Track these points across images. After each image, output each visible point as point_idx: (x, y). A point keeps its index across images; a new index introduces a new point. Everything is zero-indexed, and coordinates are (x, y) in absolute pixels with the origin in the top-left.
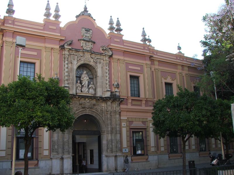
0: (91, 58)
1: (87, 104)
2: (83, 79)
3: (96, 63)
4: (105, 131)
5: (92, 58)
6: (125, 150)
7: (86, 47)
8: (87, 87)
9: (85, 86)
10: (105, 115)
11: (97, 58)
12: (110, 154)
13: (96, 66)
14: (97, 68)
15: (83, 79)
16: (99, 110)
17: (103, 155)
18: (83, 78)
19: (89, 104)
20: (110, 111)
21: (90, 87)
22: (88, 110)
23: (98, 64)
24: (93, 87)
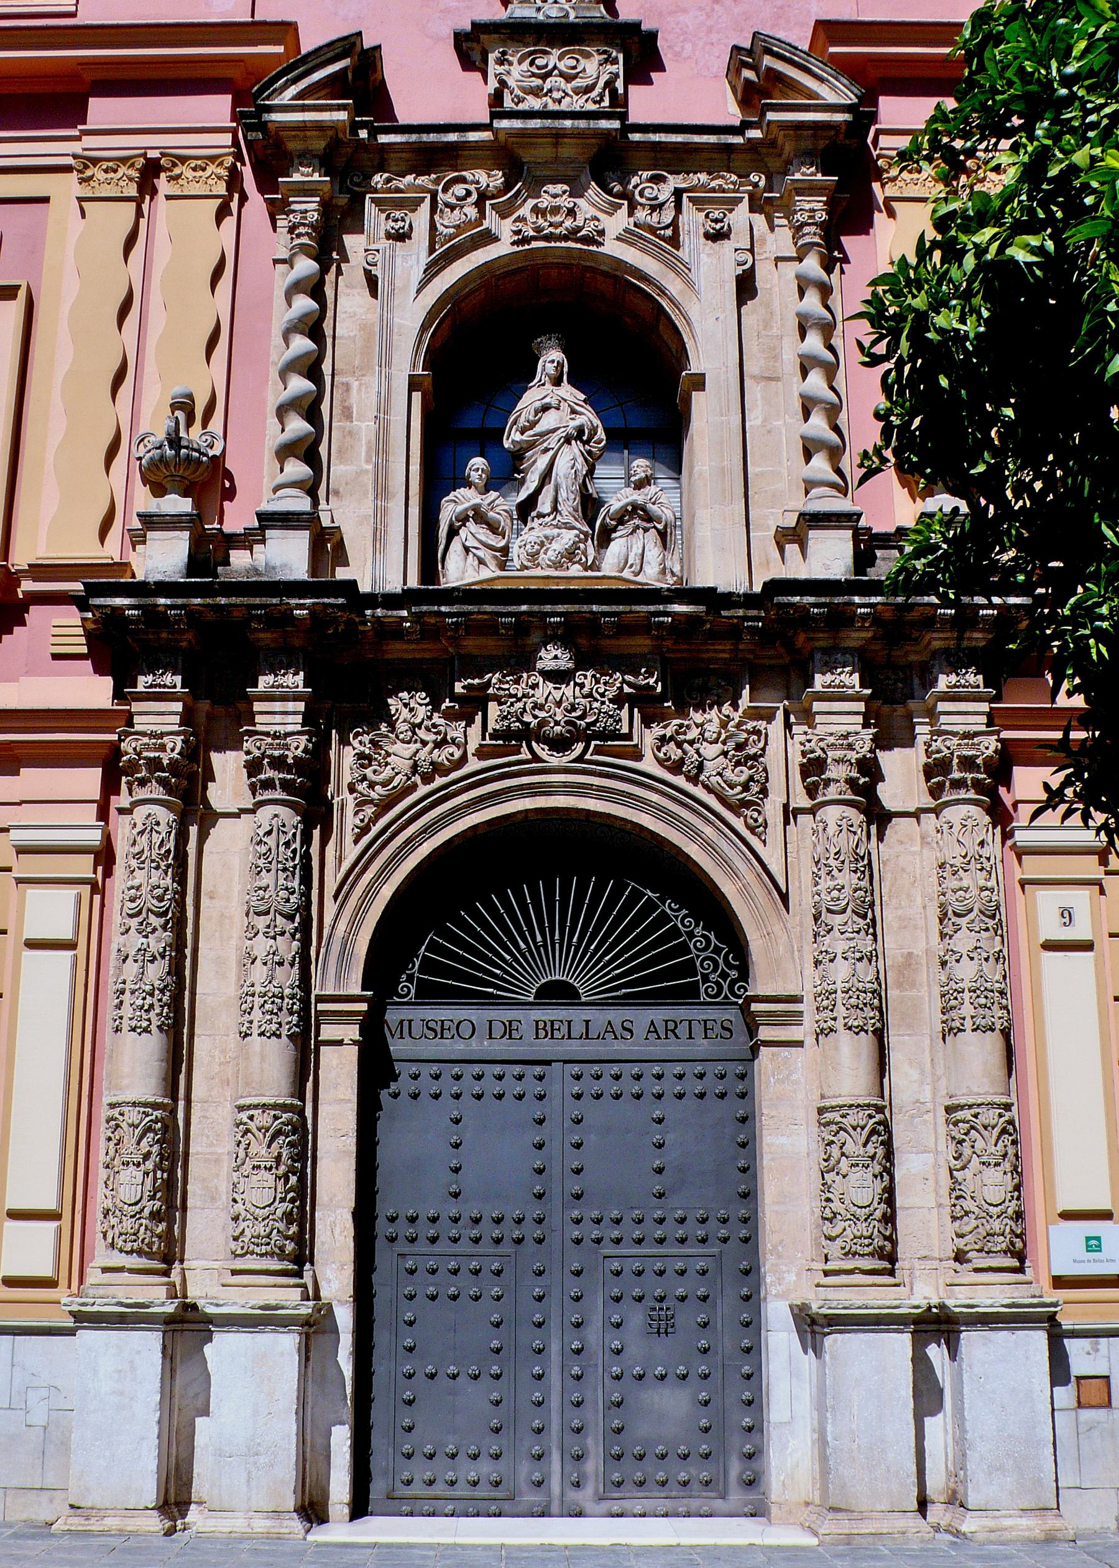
1: (546, 689)
4: (796, 999)
7: (536, 92)
9: (544, 504)
10: (789, 814)
11: (678, 193)
13: (681, 269)
14: (689, 284)
16: (710, 751)
21: (622, 518)
22: (555, 760)
23: (693, 244)
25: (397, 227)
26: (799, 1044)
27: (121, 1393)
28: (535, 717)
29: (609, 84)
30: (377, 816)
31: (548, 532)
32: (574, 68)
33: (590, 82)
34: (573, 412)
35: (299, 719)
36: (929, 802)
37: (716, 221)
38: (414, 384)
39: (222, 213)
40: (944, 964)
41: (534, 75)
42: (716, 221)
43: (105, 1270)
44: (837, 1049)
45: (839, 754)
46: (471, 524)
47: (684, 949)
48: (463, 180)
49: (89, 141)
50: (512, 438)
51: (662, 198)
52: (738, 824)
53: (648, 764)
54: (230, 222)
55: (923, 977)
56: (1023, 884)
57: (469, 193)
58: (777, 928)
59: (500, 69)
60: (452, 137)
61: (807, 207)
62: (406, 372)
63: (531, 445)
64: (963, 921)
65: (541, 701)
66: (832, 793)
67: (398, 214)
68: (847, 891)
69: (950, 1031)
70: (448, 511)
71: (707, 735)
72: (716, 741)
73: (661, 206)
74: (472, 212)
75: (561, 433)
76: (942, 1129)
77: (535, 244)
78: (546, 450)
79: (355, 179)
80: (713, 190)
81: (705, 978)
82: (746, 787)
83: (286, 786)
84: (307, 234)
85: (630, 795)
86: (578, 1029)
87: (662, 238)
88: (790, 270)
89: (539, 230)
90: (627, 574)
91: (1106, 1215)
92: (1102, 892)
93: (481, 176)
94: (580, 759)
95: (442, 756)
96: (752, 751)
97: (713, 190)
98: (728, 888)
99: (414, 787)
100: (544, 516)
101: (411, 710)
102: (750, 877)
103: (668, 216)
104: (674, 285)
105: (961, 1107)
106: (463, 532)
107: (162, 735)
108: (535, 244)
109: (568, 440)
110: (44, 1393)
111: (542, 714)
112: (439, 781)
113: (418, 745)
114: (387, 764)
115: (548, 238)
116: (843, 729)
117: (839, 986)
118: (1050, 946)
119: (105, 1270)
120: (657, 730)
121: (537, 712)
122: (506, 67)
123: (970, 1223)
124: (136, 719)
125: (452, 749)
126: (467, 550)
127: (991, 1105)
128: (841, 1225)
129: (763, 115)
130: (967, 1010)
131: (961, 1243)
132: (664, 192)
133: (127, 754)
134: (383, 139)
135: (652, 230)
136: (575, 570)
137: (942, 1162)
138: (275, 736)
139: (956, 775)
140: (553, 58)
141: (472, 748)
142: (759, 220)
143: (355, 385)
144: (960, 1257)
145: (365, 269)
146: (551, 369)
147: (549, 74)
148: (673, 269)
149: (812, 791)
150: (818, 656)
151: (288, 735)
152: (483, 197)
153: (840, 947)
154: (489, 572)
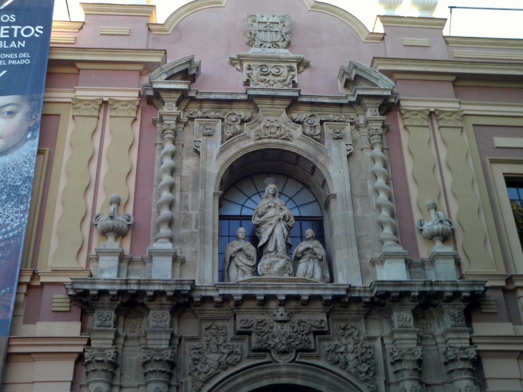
0: (294, 121)
2: (262, 219)
3: (319, 139)
5: (299, 122)
9: (271, 247)
11: (322, 122)
14: (328, 158)
15: (262, 219)
18: (260, 216)
19: (287, 328)
20: (413, 354)
21: (303, 254)
22: (283, 360)
24: (317, 250)
25: (208, 132)
28: (273, 341)
31: (273, 259)
32: (278, 72)
33: (285, 78)
34: (281, 209)
37: (338, 133)
38: (215, 194)
41: (262, 75)
42: (338, 133)
51: (315, 124)
57: (237, 120)
59: (248, 72)
61: (375, 128)
63: (264, 222)
65: (276, 334)
66: (406, 375)
71: (349, 349)
72: (352, 352)
73: (315, 127)
74: (238, 127)
75: (277, 218)
78: (271, 224)
79: (191, 113)
80: (335, 121)
84: (171, 133)
87: (316, 139)
90: (307, 277)
96: (369, 357)
97: (335, 121)
100: (271, 252)
101: (217, 338)
103: (318, 132)
104: (321, 159)
106: (236, 260)
107: (104, 349)
111: (277, 340)
113: (220, 355)
114: (206, 363)
116: (409, 346)
121: (273, 339)
122: (251, 71)
124: (93, 342)
126: (237, 266)
129: (355, 92)
132: (317, 123)
133: (87, 358)
135: (312, 136)
136: (286, 276)
141: (246, 355)
143: (190, 196)
145: (194, 149)
146: (271, 191)
147: (268, 74)
151: (162, 350)
152: (243, 122)
154: (249, 277)
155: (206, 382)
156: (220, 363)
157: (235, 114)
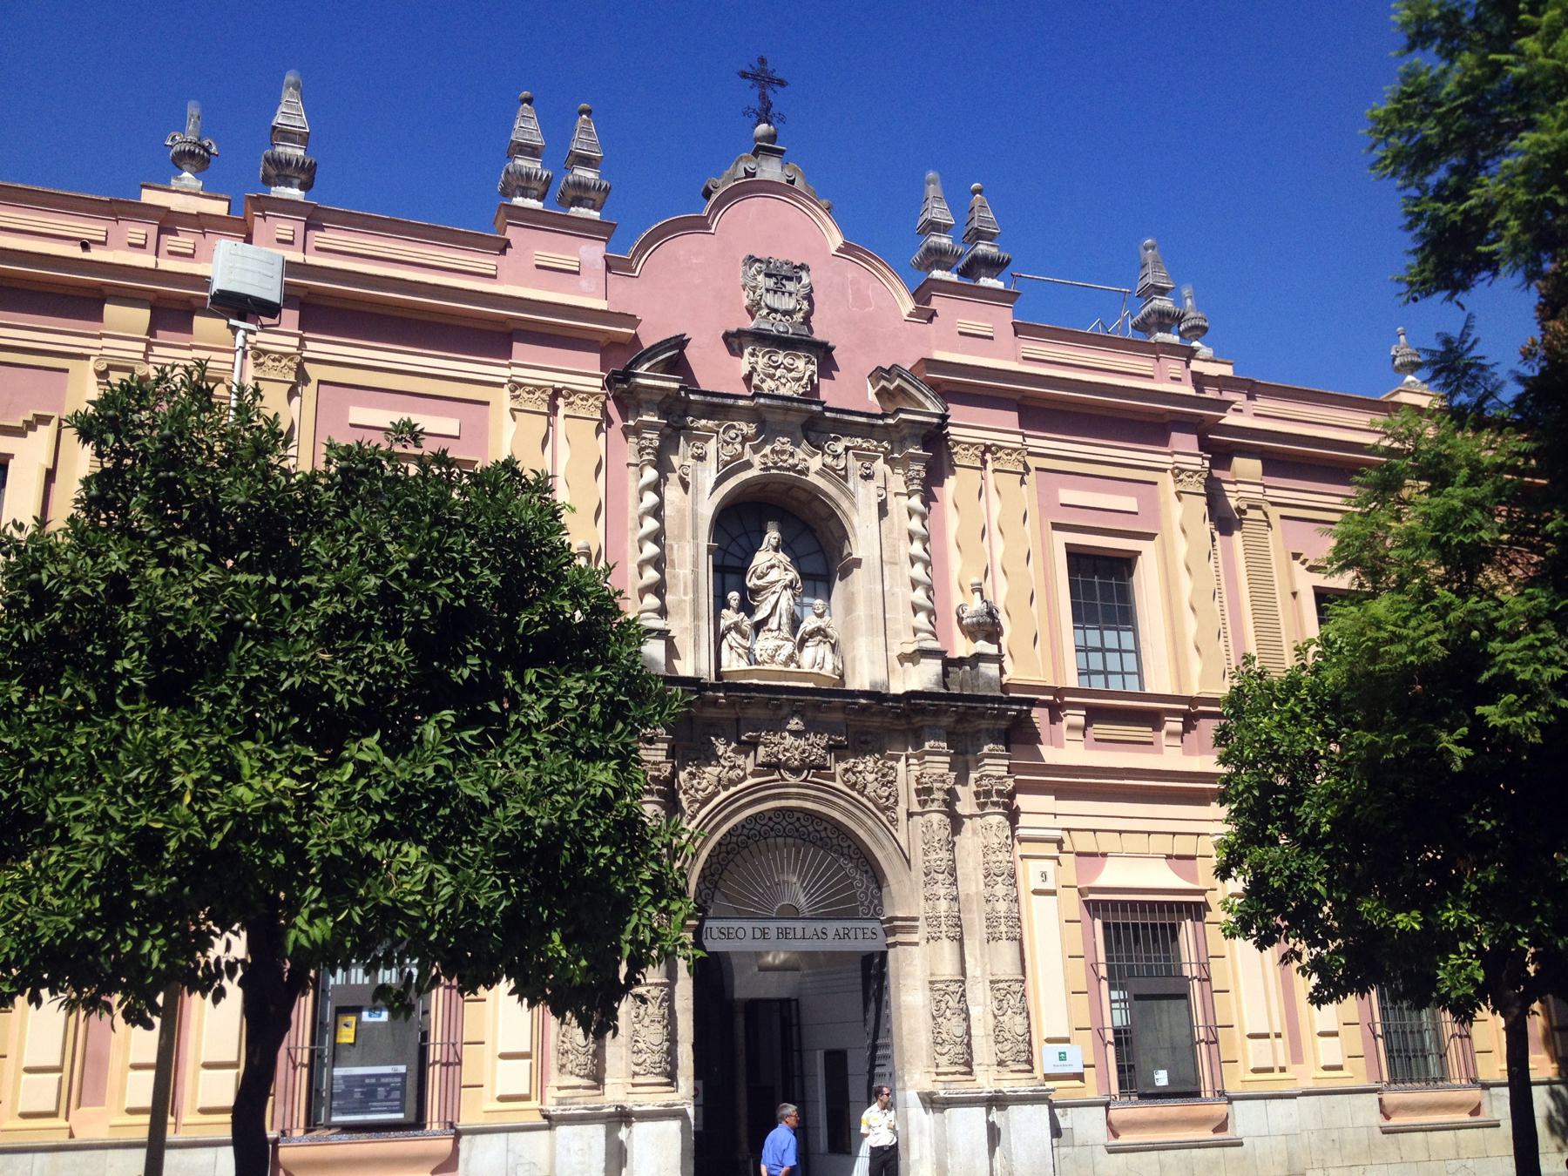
4: (915, 919)
6: (1062, 1056)
7: (772, 377)
8: (785, 628)
9: (773, 623)
10: (910, 815)
11: (847, 449)
12: (953, 1085)
13: (850, 495)
14: (854, 504)
17: (903, 1089)
18: (759, 578)
21: (812, 634)
22: (792, 780)
23: (854, 483)
26: (916, 944)
27: (583, 1163)
29: (811, 377)
30: (700, 809)
34: (786, 569)
35: (664, 753)
36: (977, 811)
39: (598, 430)
40: (988, 901)
43: (559, 1088)
44: (942, 948)
45: (939, 785)
46: (733, 633)
47: (851, 886)
48: (734, 427)
49: (515, 371)
50: (752, 582)
52: (884, 818)
53: (839, 784)
54: (602, 435)
55: (975, 907)
56: (1022, 857)
58: (905, 878)
59: (753, 360)
60: (730, 401)
62: (706, 543)
64: (1000, 879)
66: (935, 806)
67: (698, 444)
68: (945, 861)
69: (992, 938)
70: (724, 624)
74: (739, 447)
75: (782, 583)
76: (989, 993)
77: (773, 471)
80: (864, 449)
81: (862, 904)
82: (888, 799)
83: (659, 792)
85: (830, 801)
86: (799, 934)
88: (904, 500)
89: (775, 463)
91: (1067, 1041)
92: (1059, 864)
93: (743, 426)
94: (805, 780)
95: (733, 774)
97: (864, 449)
98: (879, 855)
99: (719, 792)
102: (891, 849)
104: (845, 504)
105: (998, 982)
108: (773, 471)
109: (785, 587)
110: (527, 1167)
111: (788, 754)
112: (733, 790)
115: (778, 468)
117: (943, 914)
118: (1036, 892)
119: (559, 1088)
120: (843, 765)
123: (1007, 1046)
125: (739, 771)
126: (731, 648)
127: (1017, 981)
128: (948, 1047)
130: (1003, 928)
131: (1003, 1056)
134: (692, 397)
135: (834, 470)
137: (988, 1009)
138: (654, 763)
139: (995, 799)
140: (780, 357)
142: (887, 468)
143: (676, 546)
144: (1001, 1063)
146: (774, 542)
147: (779, 367)
148: (844, 493)
149: (923, 803)
150: (926, 730)
152: (745, 439)
153: (942, 892)
155: (704, 803)
156: (720, 780)
157: (734, 427)
